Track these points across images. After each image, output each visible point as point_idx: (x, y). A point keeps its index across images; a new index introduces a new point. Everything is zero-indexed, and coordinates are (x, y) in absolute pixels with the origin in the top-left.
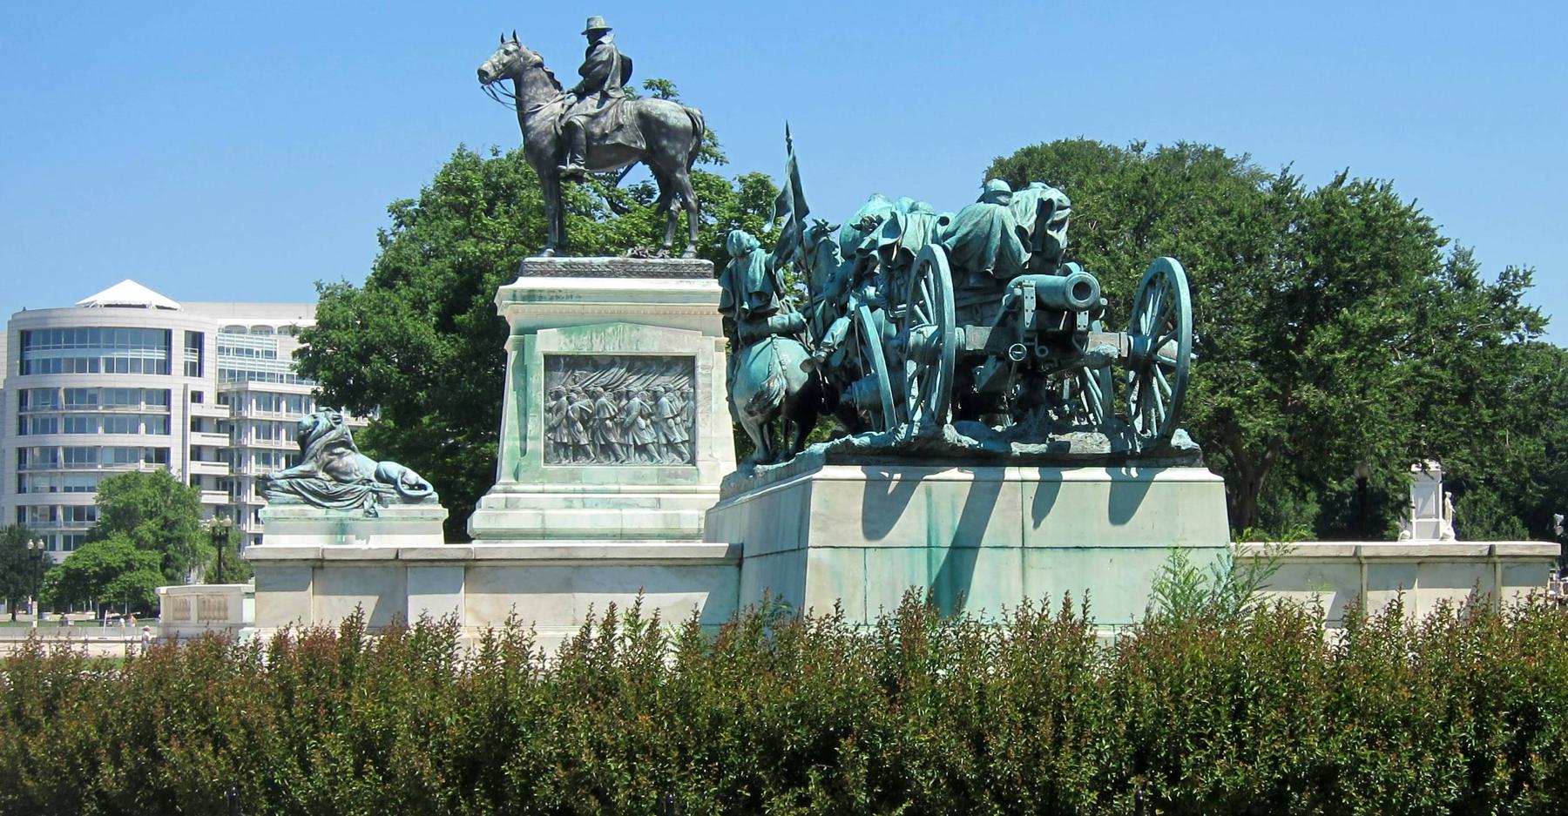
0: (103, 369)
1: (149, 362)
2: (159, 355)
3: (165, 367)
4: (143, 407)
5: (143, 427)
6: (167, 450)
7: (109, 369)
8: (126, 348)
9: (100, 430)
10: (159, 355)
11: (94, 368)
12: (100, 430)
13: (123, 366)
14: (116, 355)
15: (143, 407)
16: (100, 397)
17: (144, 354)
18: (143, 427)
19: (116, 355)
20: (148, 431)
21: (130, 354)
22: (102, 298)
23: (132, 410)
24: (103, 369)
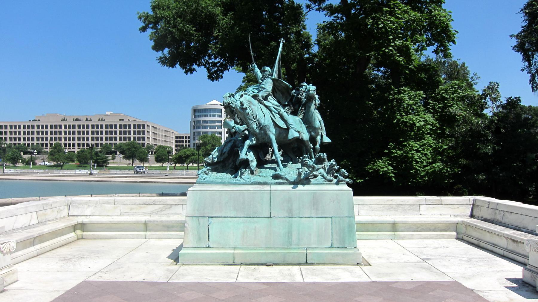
0: (209, 116)
1: (218, 115)
2: (220, 114)
3: (221, 116)
4: (217, 124)
5: (217, 128)
6: (221, 132)
7: (210, 117)
8: (213, 112)
9: (209, 128)
10: (220, 114)
11: (207, 116)
12: (209, 128)
13: (213, 116)
14: (211, 114)
15: (217, 124)
16: (209, 122)
17: (217, 114)
18: (217, 128)
19: (211, 114)
20: (218, 128)
21: (214, 114)
22: (209, 103)
23: (215, 124)
24: (209, 116)
